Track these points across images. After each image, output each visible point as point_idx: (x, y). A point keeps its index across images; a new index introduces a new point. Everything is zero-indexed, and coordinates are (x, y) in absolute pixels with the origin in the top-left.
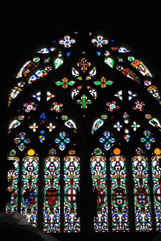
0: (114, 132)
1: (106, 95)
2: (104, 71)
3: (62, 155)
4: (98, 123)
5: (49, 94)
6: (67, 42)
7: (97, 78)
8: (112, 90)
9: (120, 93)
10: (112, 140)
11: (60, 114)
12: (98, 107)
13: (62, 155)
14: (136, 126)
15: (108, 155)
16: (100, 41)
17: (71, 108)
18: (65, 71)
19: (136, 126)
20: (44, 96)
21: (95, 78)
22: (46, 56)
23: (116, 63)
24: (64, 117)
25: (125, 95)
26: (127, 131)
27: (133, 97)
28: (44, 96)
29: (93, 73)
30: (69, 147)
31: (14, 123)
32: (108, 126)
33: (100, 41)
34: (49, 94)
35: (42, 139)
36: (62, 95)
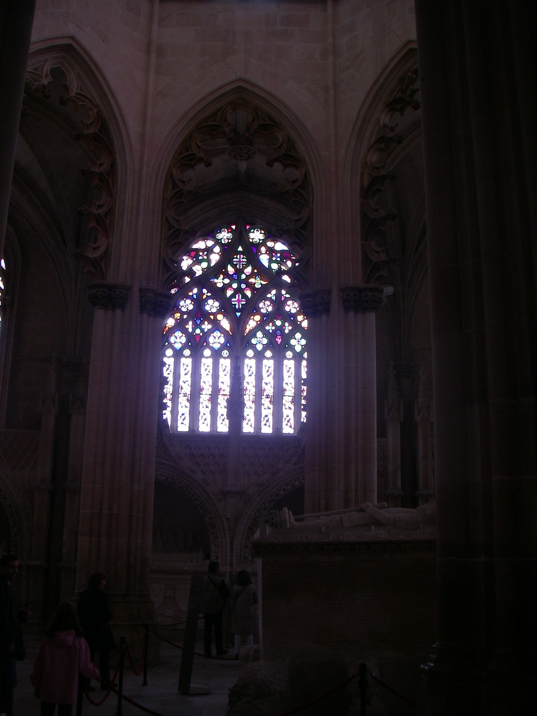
0: (266, 334)
1: (260, 294)
4: (252, 324)
6: (225, 236)
8: (265, 290)
9: (274, 292)
10: (265, 341)
12: (251, 308)
15: (259, 356)
17: (226, 308)
21: (248, 277)
23: (270, 261)
29: (249, 270)
31: (170, 322)
33: (256, 236)
34: (205, 291)
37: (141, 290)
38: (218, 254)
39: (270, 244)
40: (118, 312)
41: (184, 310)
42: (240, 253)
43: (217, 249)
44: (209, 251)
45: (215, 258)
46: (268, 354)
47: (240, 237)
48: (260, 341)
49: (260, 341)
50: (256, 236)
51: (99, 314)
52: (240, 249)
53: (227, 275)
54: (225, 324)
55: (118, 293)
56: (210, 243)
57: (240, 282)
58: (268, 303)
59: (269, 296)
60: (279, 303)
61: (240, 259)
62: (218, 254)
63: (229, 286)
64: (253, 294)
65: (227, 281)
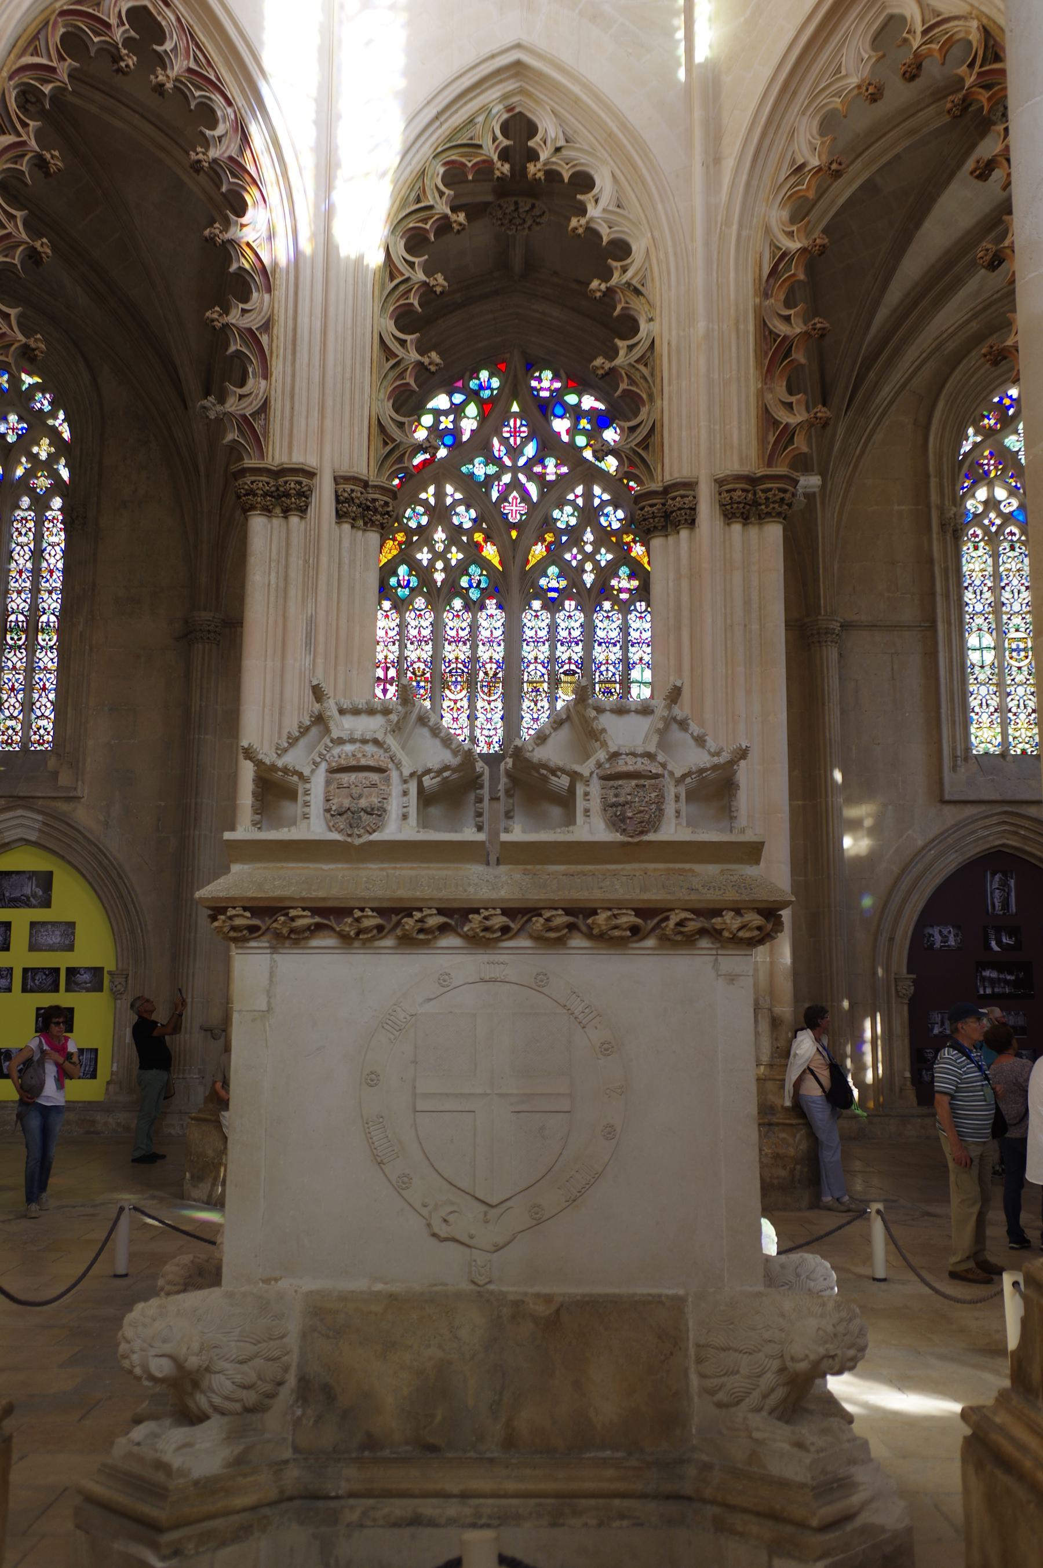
1: (554, 492)
2: (549, 444)
3: (473, 607)
5: (449, 489)
7: (539, 459)
11: (470, 532)
13: (473, 607)
14: (605, 557)
16: (546, 382)
18: (480, 445)
19: (605, 557)
20: (440, 495)
22: (446, 413)
24: (478, 537)
25: (588, 495)
26: (588, 566)
27: (602, 501)
28: (440, 495)
29: (530, 450)
30: (486, 594)
32: (553, 555)
34: (449, 489)
35: (439, 577)
36: (475, 492)
37: (336, 480)
38: (475, 418)
39: (571, 399)
40: (294, 520)
41: (413, 524)
42: (515, 415)
43: (472, 410)
44: (457, 410)
45: (468, 426)
46: (570, 605)
47: (516, 387)
48: (552, 579)
49: (552, 579)
50: (546, 382)
51: (258, 523)
52: (515, 408)
53: (491, 459)
54: (490, 552)
55: (292, 485)
56: (458, 398)
57: (515, 470)
58: (568, 509)
59: (571, 497)
60: (589, 514)
61: (516, 428)
62: (475, 418)
63: (497, 476)
64: (542, 495)
65: (492, 470)
